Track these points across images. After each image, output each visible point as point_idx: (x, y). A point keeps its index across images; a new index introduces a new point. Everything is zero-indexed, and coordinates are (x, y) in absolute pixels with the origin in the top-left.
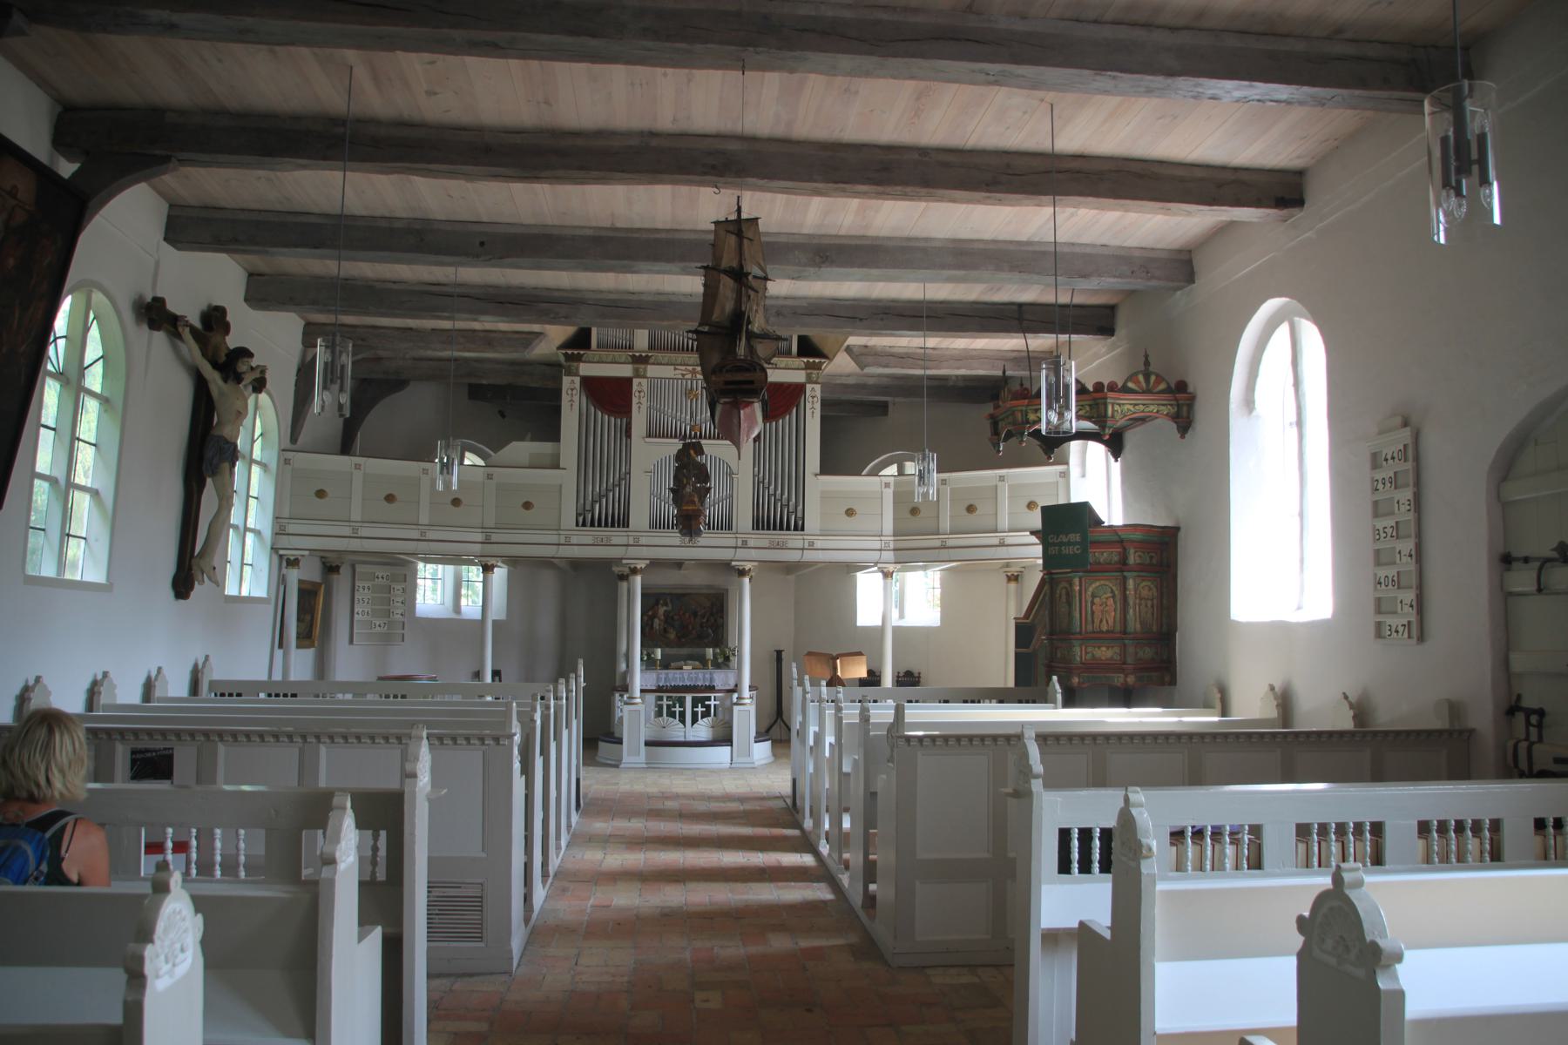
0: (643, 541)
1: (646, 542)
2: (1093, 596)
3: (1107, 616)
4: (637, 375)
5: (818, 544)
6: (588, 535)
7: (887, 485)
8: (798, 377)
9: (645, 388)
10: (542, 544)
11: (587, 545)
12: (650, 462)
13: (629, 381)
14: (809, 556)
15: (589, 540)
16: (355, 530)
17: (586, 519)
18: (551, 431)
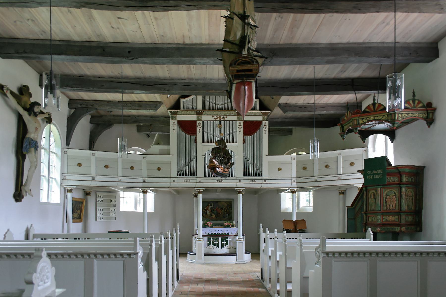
0: (202, 181)
1: (203, 180)
2: (386, 195)
3: (393, 205)
6: (182, 179)
7: (294, 159)
8: (260, 118)
9: (201, 124)
10: (164, 183)
11: (181, 182)
12: (204, 151)
13: (195, 122)
14: (264, 186)
15: (182, 181)
16: (93, 178)
17: (180, 174)
18: (166, 140)
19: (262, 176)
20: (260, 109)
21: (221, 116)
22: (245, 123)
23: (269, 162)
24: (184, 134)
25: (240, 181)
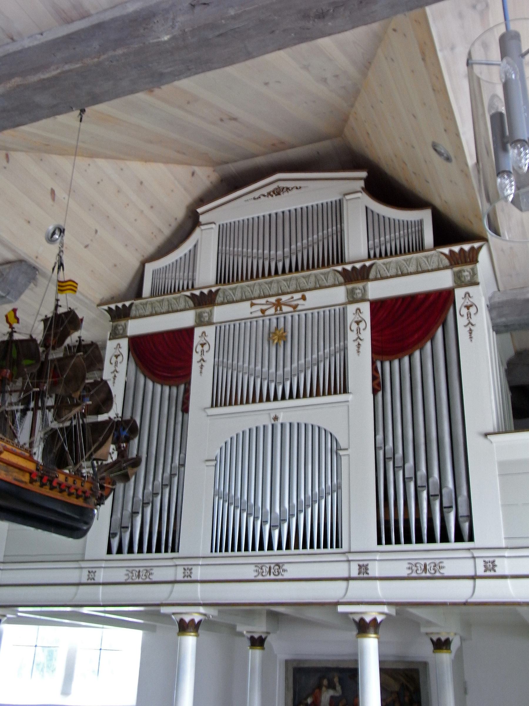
0: (198, 573)
4: (200, 322)
5: (504, 567)
8: (443, 280)
9: (211, 339)
13: (189, 332)
14: (488, 591)
19: (471, 539)
20: (439, 242)
21: (284, 298)
22: (377, 306)
23: (501, 464)
24: (150, 384)
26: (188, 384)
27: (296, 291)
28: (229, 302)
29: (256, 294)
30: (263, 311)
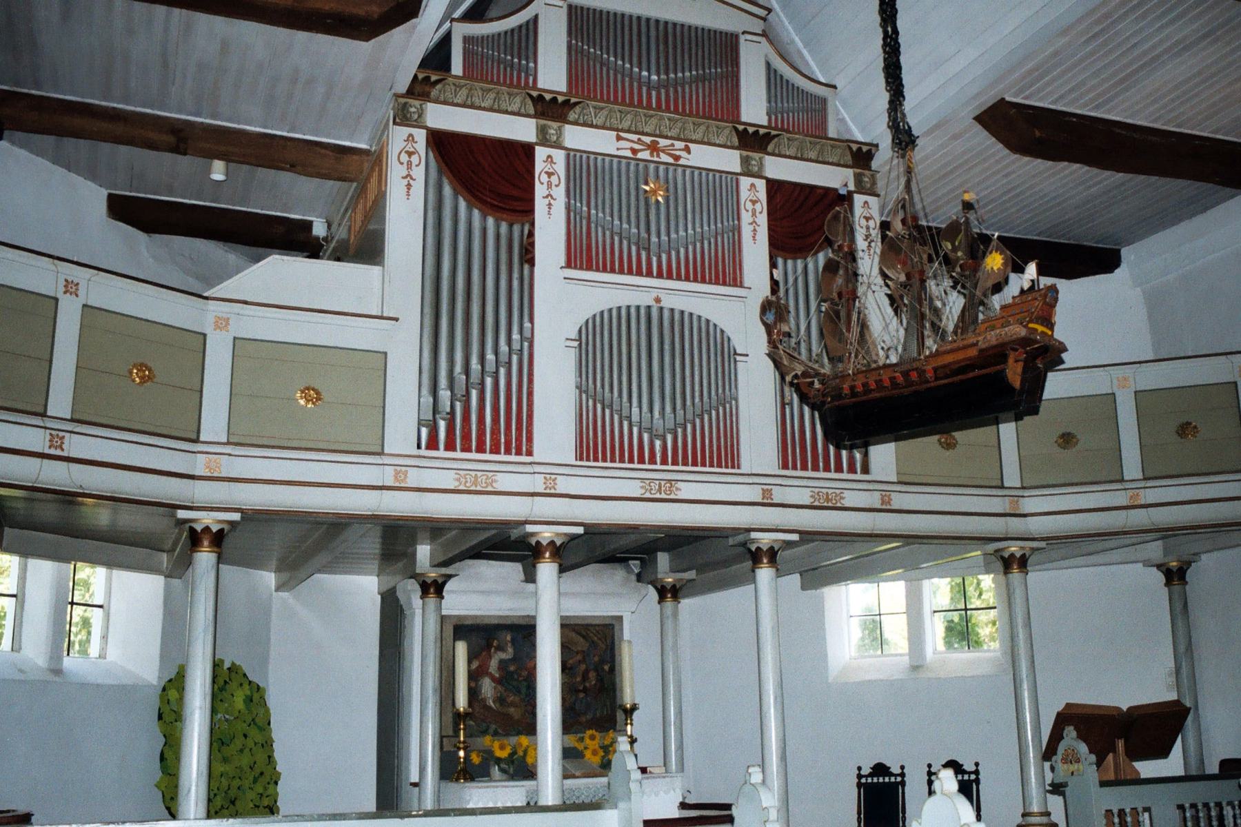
4: (544, 141)
6: (444, 470)
9: (560, 168)
13: (527, 150)
15: (447, 480)
21: (663, 142)
22: (775, 188)
25: (767, 493)
26: (533, 224)
27: (678, 139)
28: (585, 125)
29: (626, 125)
30: (634, 151)
